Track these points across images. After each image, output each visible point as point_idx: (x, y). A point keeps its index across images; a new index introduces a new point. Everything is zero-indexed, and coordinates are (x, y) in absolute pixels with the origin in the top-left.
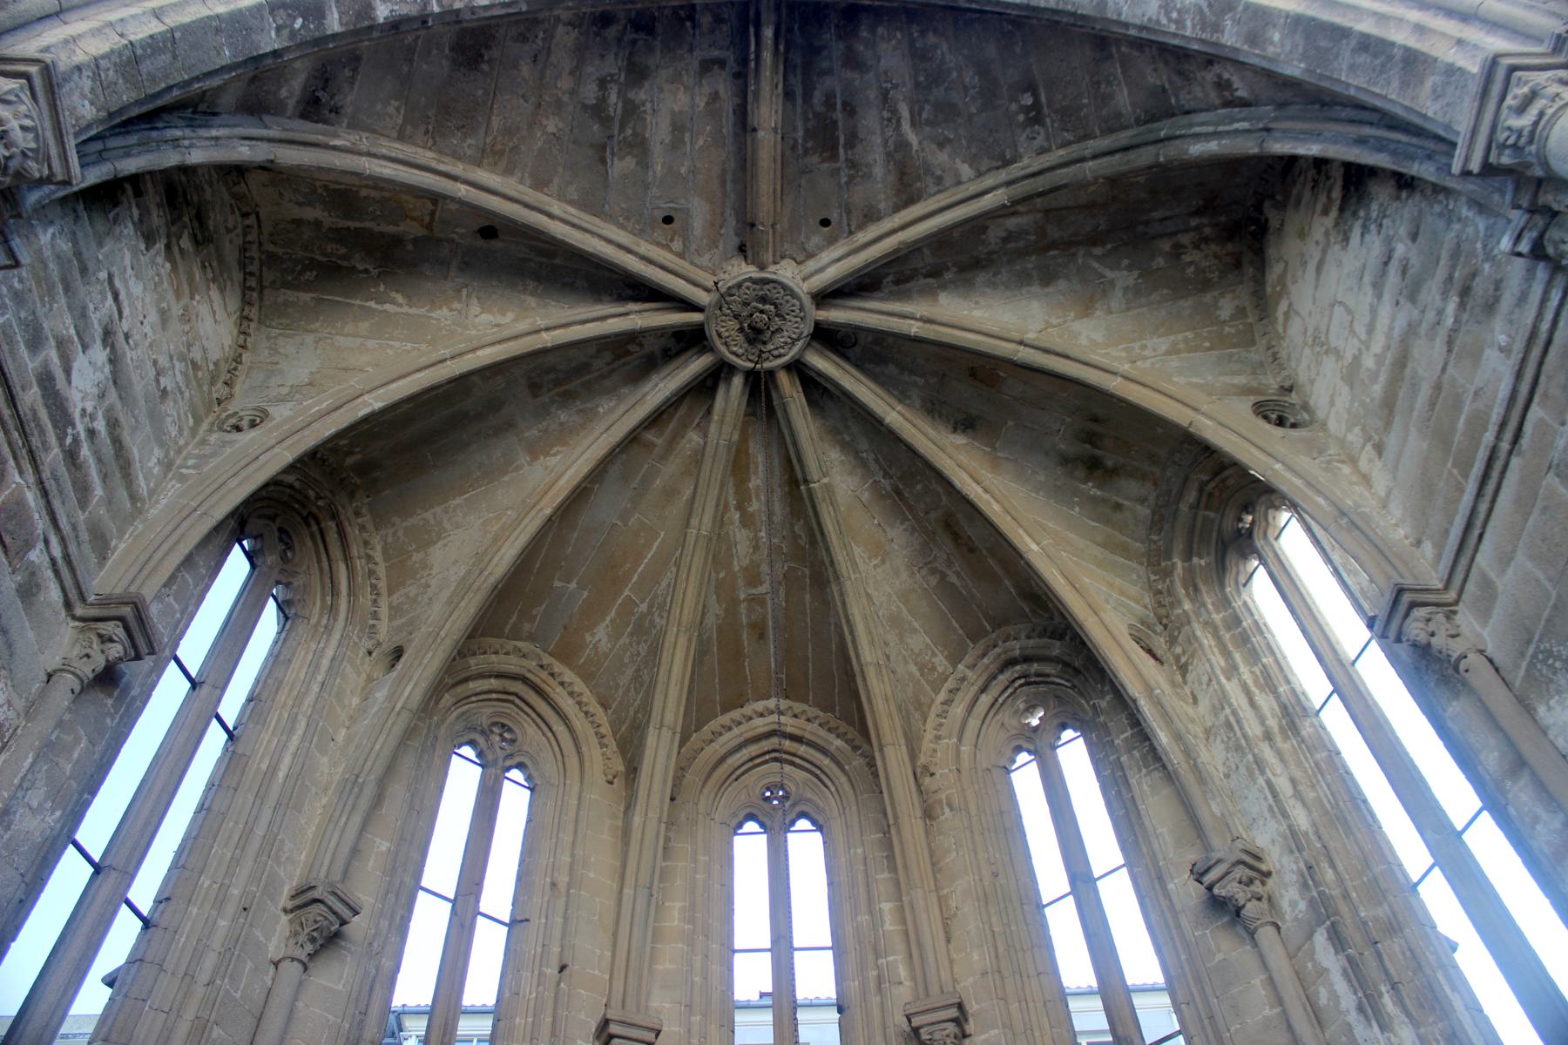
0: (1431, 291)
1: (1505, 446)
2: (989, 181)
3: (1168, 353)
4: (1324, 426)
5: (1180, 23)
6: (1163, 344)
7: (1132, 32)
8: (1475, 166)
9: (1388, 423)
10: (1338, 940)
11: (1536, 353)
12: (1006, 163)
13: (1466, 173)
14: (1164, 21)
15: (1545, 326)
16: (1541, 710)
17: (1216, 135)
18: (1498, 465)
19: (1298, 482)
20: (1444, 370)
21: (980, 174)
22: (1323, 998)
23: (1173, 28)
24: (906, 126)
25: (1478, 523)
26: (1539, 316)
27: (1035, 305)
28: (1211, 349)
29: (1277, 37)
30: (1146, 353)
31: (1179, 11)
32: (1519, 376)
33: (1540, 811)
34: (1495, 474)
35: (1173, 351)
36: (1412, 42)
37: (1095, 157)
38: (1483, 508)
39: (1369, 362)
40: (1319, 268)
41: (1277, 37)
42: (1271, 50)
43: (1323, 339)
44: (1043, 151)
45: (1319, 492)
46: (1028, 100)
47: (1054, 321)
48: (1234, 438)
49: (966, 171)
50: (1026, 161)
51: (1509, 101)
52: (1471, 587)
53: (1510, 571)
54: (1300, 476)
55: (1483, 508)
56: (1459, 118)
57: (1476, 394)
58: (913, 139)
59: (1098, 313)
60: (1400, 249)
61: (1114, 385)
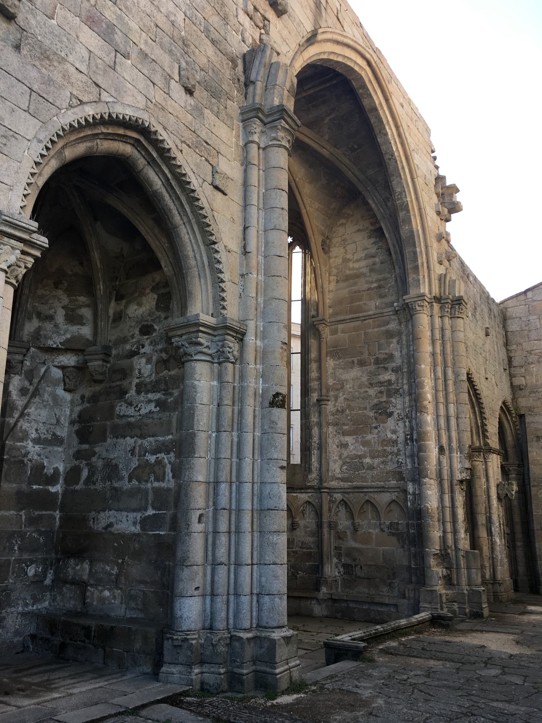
0: (375, 277)
1: (361, 319)
2: (328, 147)
3: (317, 210)
4: (330, 258)
5: (398, 199)
6: (317, 205)
7: (390, 184)
8: (406, 301)
9: (344, 281)
11: (380, 315)
12: (335, 147)
13: (404, 300)
14: (397, 194)
15: (385, 314)
16: (328, 358)
17: (376, 204)
18: (357, 319)
19: (319, 272)
20: (363, 291)
21: (328, 141)
23: (396, 197)
24: (329, 118)
25: (345, 322)
26: (386, 312)
27: (303, 170)
28: (323, 214)
29: (407, 228)
30: (313, 206)
31: (401, 197)
32: (374, 314)
33: (315, 371)
34: (355, 320)
35: (317, 210)
36: (420, 264)
37: (352, 173)
38: (348, 321)
39: (351, 265)
40: (359, 230)
41: (407, 228)
42: (404, 227)
43: (346, 243)
44: (345, 155)
45: (321, 278)
46: (356, 147)
47: (304, 179)
48: (315, 249)
49: (326, 137)
50: (339, 152)
51: (419, 302)
52: (333, 327)
53: (343, 334)
54: (321, 271)
55: (348, 321)
56: (413, 292)
57: (365, 304)
58: (327, 121)
59: (313, 185)
60: (377, 260)
61: (304, 211)
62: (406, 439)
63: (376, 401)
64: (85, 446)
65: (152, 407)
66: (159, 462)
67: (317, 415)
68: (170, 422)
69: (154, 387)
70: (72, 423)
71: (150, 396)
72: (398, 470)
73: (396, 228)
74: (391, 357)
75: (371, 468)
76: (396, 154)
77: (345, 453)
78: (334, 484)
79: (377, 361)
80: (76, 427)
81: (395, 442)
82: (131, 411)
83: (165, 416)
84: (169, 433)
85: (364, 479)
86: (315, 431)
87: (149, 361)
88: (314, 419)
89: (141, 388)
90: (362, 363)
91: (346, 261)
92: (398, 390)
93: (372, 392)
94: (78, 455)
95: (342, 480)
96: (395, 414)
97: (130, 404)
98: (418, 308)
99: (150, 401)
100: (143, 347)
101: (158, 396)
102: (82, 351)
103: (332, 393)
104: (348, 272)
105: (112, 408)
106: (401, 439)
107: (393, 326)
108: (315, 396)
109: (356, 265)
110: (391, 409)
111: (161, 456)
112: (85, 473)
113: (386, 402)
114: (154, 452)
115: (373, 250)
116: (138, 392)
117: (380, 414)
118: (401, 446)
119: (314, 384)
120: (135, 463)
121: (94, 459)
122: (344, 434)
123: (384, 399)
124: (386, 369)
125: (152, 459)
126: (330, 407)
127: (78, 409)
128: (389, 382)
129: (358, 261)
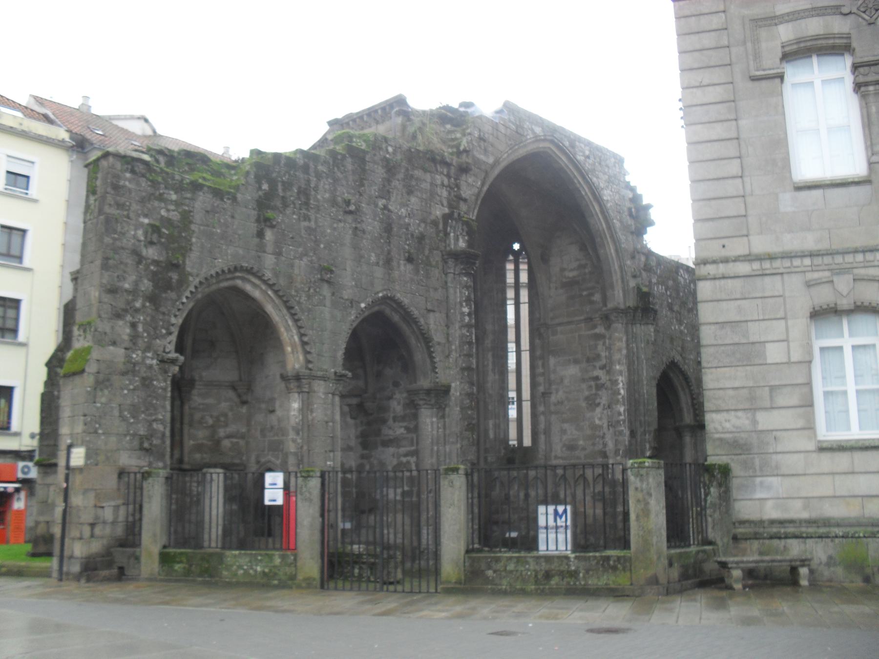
10: (493, 356)
22: (486, 363)
36: (615, 282)
62: (608, 426)
63: (587, 393)
64: (365, 452)
65: (402, 430)
66: (408, 462)
67: (543, 405)
68: (412, 439)
69: (403, 418)
70: (357, 437)
71: (401, 424)
72: (603, 450)
73: (595, 250)
74: (598, 357)
75: (584, 449)
76: (586, 197)
77: (565, 437)
78: (554, 462)
79: (588, 360)
80: (360, 440)
81: (601, 427)
82: (391, 432)
83: (410, 436)
84: (412, 445)
85: (578, 458)
86: (542, 418)
87: (399, 403)
88: (541, 409)
89: (395, 419)
90: (576, 362)
91: (563, 270)
92: (604, 385)
93: (584, 386)
94: (363, 457)
95: (562, 458)
96: (602, 404)
97: (390, 428)
98: (613, 318)
99: (401, 427)
100: (395, 394)
101: (405, 424)
102: (360, 396)
103: (554, 387)
104: (564, 280)
105: (380, 430)
106: (605, 425)
107: (600, 330)
108: (541, 389)
109: (571, 274)
110: (598, 401)
111: (409, 458)
112: (367, 467)
113: (596, 394)
114: (406, 455)
115: (583, 262)
116: (394, 421)
117: (591, 405)
118: (605, 430)
119: (541, 379)
120: (395, 462)
121: (372, 459)
122: (564, 421)
123: (594, 391)
124: (595, 367)
125: (404, 460)
126: (553, 398)
127: (360, 429)
128: (597, 378)
129: (572, 270)
